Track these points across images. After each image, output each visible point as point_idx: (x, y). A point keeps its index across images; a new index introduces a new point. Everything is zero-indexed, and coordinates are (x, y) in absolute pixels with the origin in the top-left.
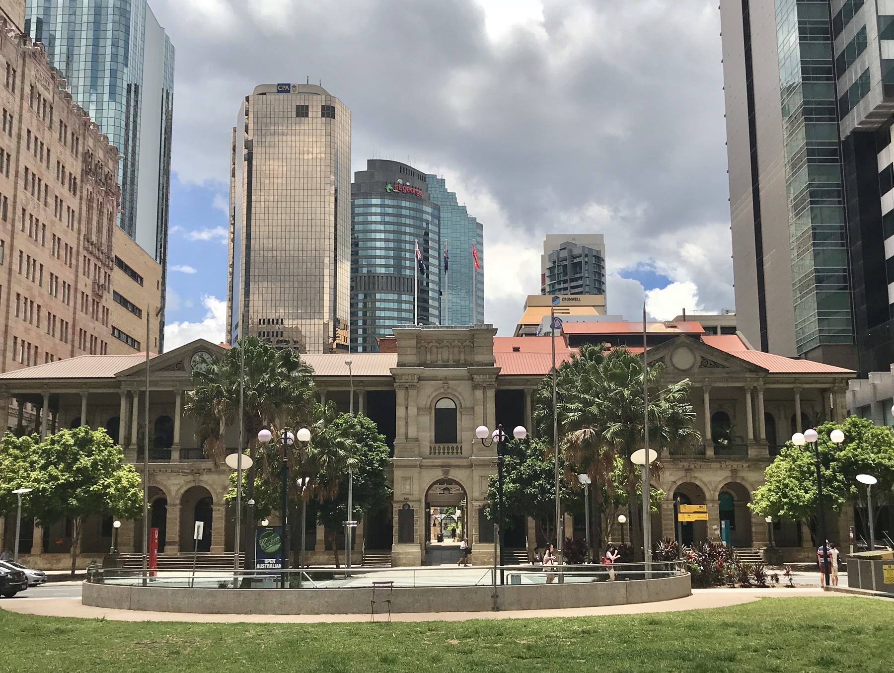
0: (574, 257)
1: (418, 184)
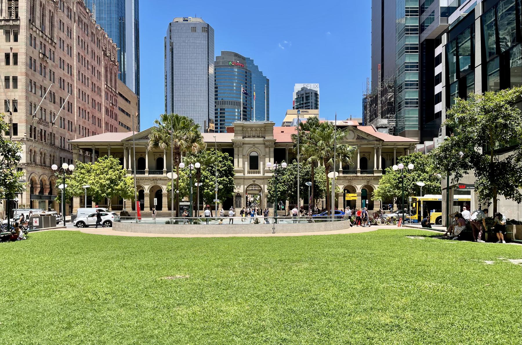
0: (306, 94)
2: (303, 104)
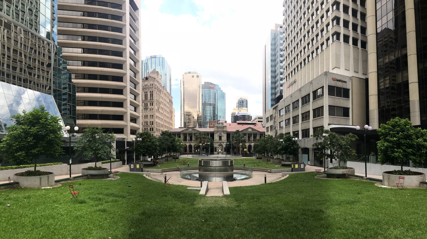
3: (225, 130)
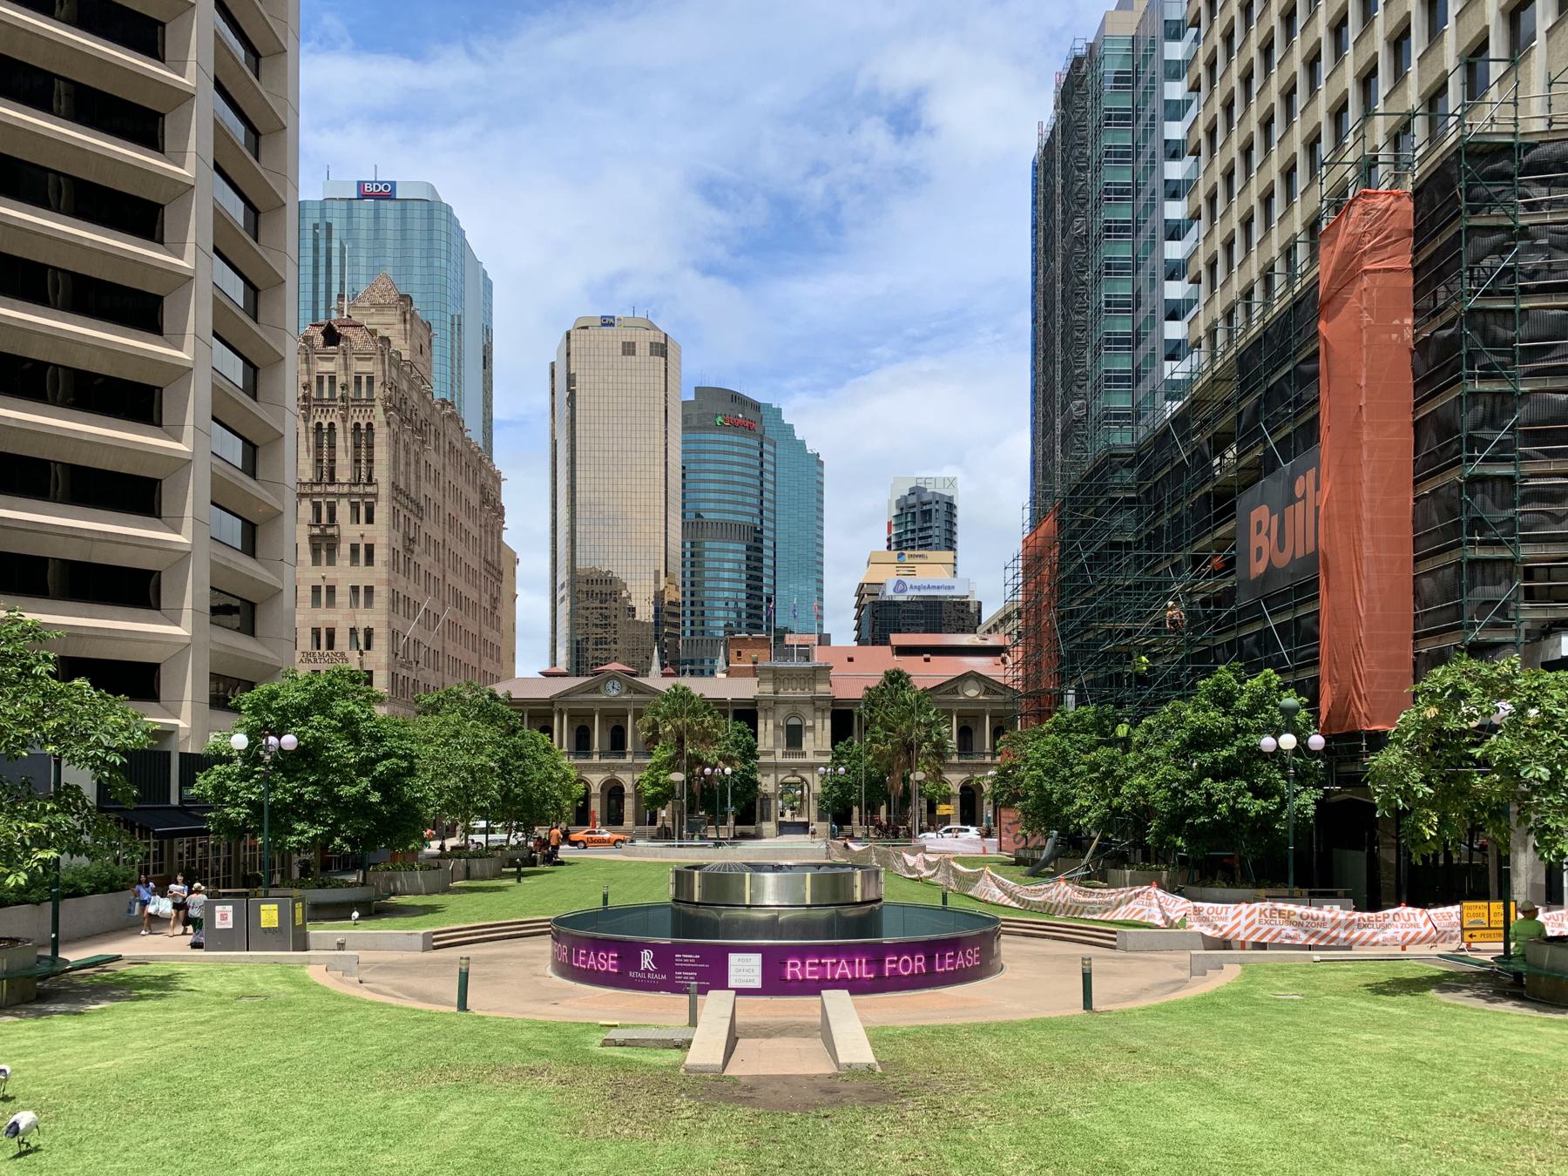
0: (924, 504)
1: (751, 415)
2: (913, 531)
3: (822, 689)
